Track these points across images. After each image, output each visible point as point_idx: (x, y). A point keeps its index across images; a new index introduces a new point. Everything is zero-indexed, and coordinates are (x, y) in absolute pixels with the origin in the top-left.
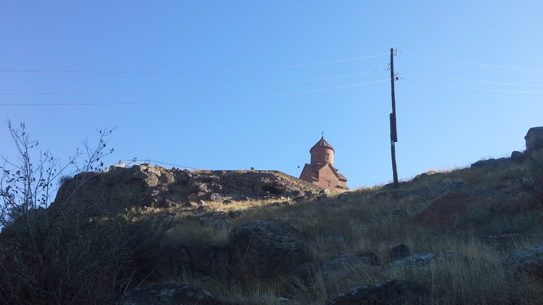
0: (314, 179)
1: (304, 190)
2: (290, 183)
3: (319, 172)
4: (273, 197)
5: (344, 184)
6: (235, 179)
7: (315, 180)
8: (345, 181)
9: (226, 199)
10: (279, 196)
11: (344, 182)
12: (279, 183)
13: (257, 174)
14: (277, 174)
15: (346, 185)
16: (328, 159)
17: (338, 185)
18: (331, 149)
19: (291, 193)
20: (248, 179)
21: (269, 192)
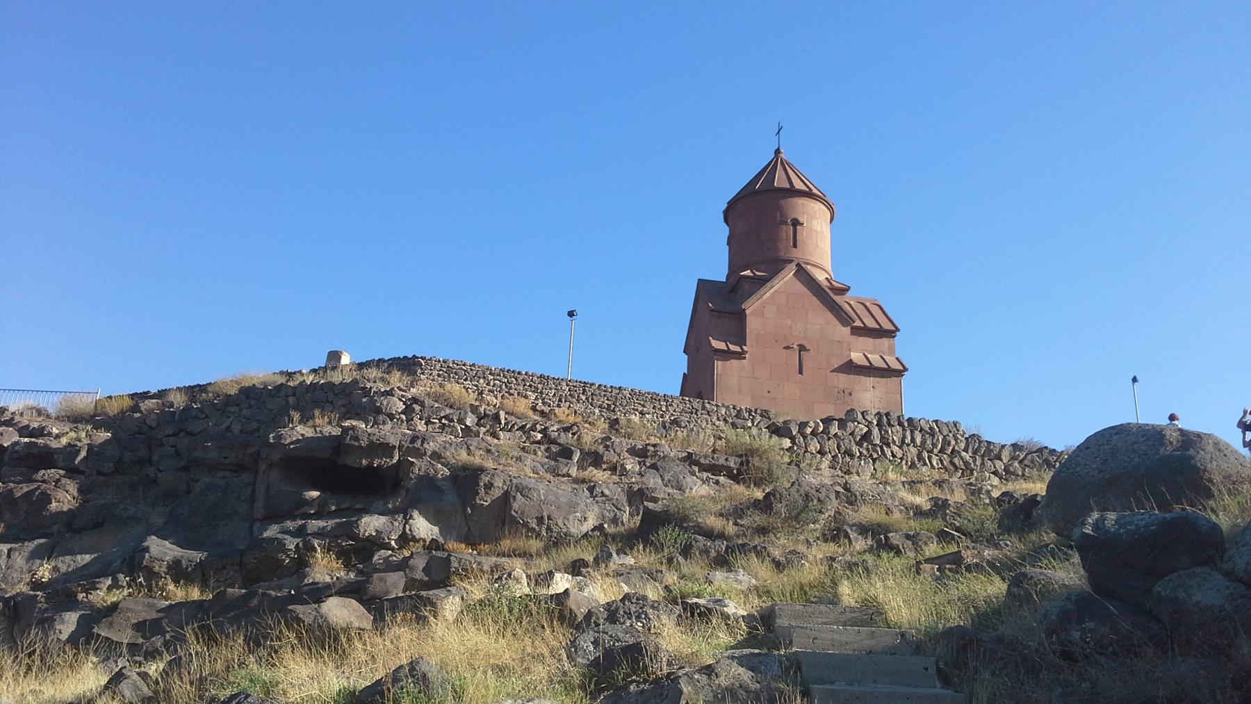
0: (717, 351)
1: (566, 439)
2: (461, 421)
3: (744, 310)
4: (315, 525)
5: (886, 349)
6: (191, 434)
7: (727, 355)
8: (891, 334)
9: (55, 569)
10: (379, 504)
12: (357, 439)
13: (282, 394)
14: (396, 379)
15: (892, 351)
16: (795, 246)
17: (851, 360)
18: (809, 194)
19: (446, 486)
20: (236, 428)
21: (315, 494)
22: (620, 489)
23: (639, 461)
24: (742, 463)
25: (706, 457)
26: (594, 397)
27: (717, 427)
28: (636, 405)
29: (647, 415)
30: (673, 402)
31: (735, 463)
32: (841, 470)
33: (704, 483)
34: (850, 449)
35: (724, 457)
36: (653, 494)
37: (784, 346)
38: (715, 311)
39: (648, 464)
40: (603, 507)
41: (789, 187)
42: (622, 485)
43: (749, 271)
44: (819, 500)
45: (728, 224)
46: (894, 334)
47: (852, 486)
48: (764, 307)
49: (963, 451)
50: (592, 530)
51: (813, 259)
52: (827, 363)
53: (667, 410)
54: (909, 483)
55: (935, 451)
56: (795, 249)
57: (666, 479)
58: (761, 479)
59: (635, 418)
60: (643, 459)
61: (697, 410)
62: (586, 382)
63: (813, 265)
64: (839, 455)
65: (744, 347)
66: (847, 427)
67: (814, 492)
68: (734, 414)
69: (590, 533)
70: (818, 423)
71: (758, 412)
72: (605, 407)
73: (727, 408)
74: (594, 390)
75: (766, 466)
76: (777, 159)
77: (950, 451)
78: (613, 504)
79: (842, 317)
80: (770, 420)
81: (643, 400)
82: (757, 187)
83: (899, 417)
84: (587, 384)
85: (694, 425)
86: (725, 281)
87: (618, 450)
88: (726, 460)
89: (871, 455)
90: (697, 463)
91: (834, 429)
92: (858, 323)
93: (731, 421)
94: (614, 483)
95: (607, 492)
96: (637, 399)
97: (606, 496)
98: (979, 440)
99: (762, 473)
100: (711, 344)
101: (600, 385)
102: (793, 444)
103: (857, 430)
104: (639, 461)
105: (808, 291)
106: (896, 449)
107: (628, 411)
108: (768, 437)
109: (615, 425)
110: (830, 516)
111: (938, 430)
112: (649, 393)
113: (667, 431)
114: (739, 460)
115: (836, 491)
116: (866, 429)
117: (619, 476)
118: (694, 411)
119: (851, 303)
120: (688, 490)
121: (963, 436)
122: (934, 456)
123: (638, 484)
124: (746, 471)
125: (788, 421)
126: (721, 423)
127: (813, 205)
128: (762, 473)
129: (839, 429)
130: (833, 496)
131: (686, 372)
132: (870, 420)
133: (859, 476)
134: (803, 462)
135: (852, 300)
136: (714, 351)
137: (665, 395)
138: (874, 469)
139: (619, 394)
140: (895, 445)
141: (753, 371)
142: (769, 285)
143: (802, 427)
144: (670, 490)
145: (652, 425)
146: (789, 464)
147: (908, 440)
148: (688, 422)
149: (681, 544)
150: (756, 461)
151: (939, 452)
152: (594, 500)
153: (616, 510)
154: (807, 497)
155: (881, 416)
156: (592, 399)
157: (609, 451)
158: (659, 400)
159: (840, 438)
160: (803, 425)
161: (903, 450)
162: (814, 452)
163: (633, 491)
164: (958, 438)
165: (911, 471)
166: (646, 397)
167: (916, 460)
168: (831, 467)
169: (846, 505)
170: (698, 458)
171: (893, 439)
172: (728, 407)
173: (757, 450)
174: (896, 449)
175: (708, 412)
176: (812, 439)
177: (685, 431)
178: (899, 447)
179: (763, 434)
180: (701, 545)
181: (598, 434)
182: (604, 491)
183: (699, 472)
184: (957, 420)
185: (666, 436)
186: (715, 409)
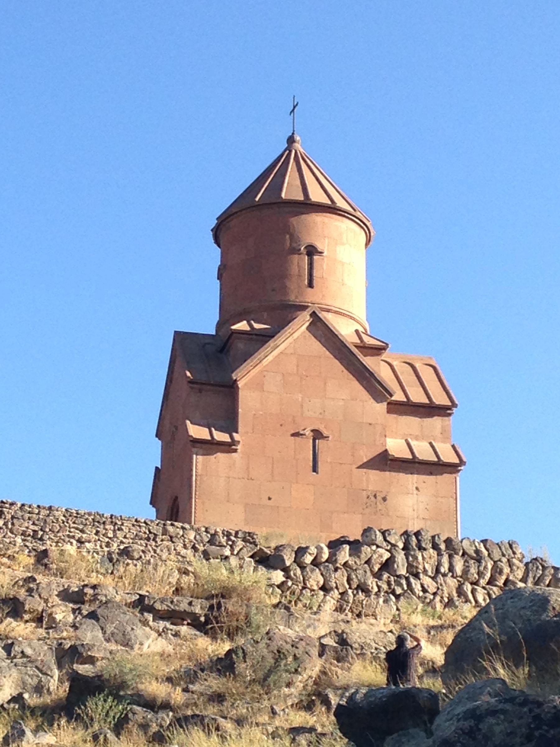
3: (236, 380)
11: (436, 422)
15: (445, 435)
17: (386, 450)
22: (46, 648)
23: (73, 609)
24: (211, 607)
25: (162, 601)
26: (15, 521)
27: (183, 557)
28: (72, 530)
29: (87, 544)
30: (122, 524)
31: (201, 608)
32: (352, 612)
33: (160, 635)
34: (365, 582)
35: (185, 602)
36: (89, 653)
37: (293, 432)
38: (196, 383)
39: (85, 612)
40: (25, 671)
41: (302, 199)
42: (49, 642)
43: (245, 322)
44: (295, 657)
45: (219, 246)
46: (449, 412)
47: (350, 636)
48: (264, 376)
49: (521, 581)
50: (9, 702)
51: (336, 304)
52: (353, 455)
53: (115, 536)
54: (433, 627)
55: (483, 582)
56: (310, 289)
57: (108, 632)
58: (237, 628)
59: (71, 549)
60: (79, 606)
61: (156, 535)
62: (4, 500)
63: (336, 312)
64: (350, 591)
65: (235, 434)
66: (360, 552)
67: (289, 647)
68: (208, 540)
69: (6, 706)
70: (322, 548)
71: (240, 535)
72: (29, 535)
73: (197, 530)
74: (15, 512)
75: (243, 610)
76: (290, 151)
77: (503, 581)
78: (37, 667)
79: (376, 388)
80: (256, 545)
81: (82, 523)
82: (257, 199)
83: (433, 537)
84: (4, 503)
85: (151, 557)
86: (214, 333)
87: (44, 595)
88: (190, 604)
89: (393, 592)
90: (150, 609)
91: (344, 555)
92: (399, 396)
93: (201, 548)
94: (39, 639)
95: (29, 651)
96: (74, 523)
97: (28, 657)
98: (543, 567)
99: (237, 620)
100: (188, 432)
101: (23, 505)
102: (287, 578)
103: (375, 556)
104: (73, 609)
105: (328, 353)
106: (427, 581)
107: (60, 539)
108: (252, 569)
109: (44, 559)
110: (310, 677)
111: (486, 553)
112: (90, 514)
113: (113, 565)
114: (207, 604)
115: (323, 644)
116: (387, 555)
117: (46, 629)
118: (152, 536)
119: (395, 363)
120: (137, 647)
121: (521, 561)
122: (479, 589)
123: (70, 639)
124: (216, 618)
125: (281, 546)
126: (189, 553)
127: (337, 223)
128: (237, 620)
129: (350, 555)
130: (315, 652)
131: (160, 467)
132: (393, 542)
133: (376, 619)
134: (296, 604)
135: (396, 359)
136: (191, 441)
137: (112, 516)
138: (398, 609)
139: (48, 516)
140: (427, 575)
141: (248, 468)
142: (272, 345)
143: (299, 555)
144: (113, 647)
145: (93, 557)
146: (276, 606)
147: (444, 569)
148: (143, 552)
149: (114, 717)
150: (230, 605)
151: (488, 583)
152: (12, 662)
153: (40, 675)
154: (279, 655)
155: (409, 536)
156: (13, 524)
157: (33, 597)
158: (104, 523)
159: (351, 568)
160: (301, 552)
161: (437, 583)
162: (315, 588)
163: (63, 649)
164: (514, 564)
165: (447, 610)
166: (86, 519)
167: (455, 594)
168: (340, 609)
169: (335, 662)
170: (152, 602)
171: (424, 568)
172: (199, 529)
173: (234, 589)
174: (427, 581)
175: (171, 537)
176: (312, 571)
177: (139, 564)
178: (433, 578)
179: (244, 566)
180: (139, 718)
181: (21, 574)
182: (25, 651)
183: (154, 620)
184: (514, 540)
185: (112, 573)
186: (181, 533)
